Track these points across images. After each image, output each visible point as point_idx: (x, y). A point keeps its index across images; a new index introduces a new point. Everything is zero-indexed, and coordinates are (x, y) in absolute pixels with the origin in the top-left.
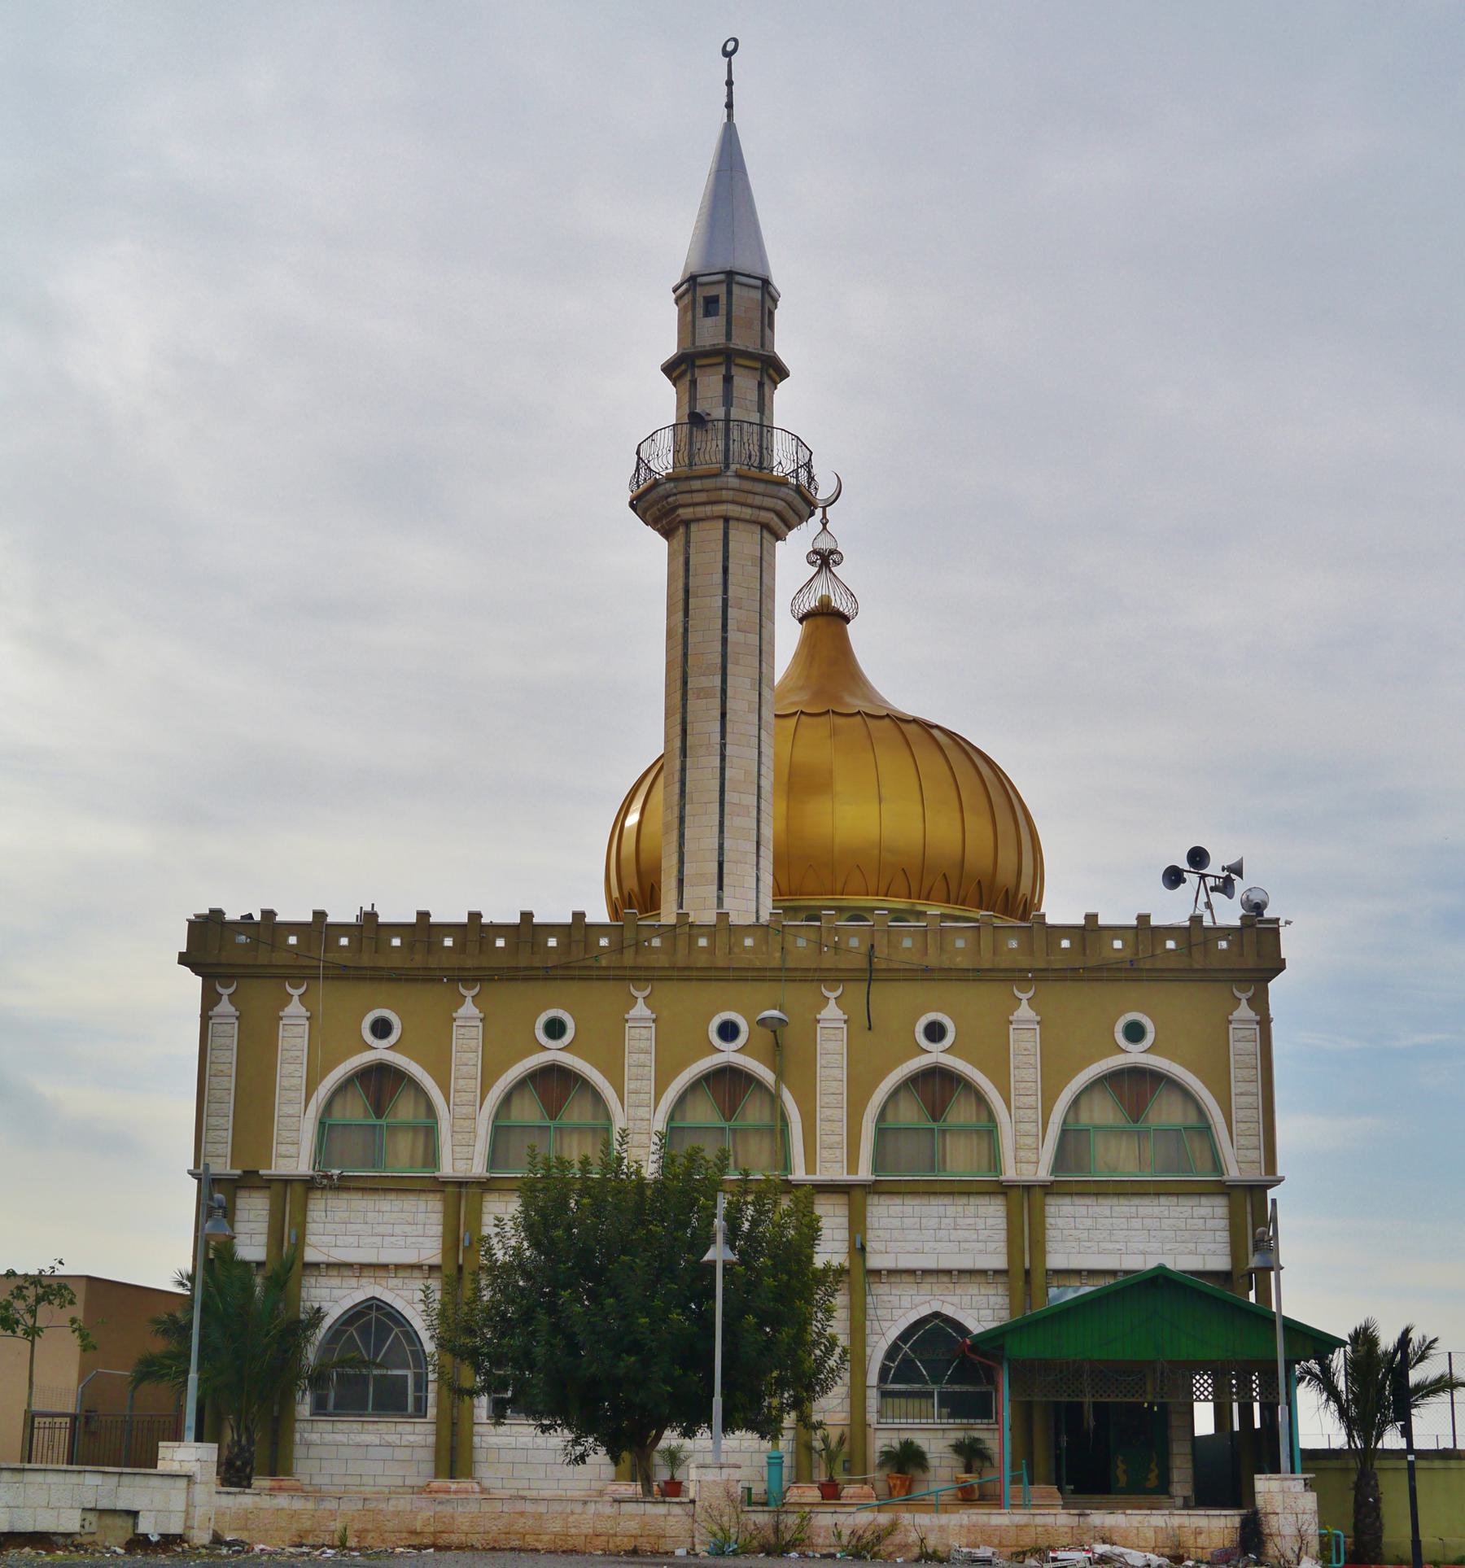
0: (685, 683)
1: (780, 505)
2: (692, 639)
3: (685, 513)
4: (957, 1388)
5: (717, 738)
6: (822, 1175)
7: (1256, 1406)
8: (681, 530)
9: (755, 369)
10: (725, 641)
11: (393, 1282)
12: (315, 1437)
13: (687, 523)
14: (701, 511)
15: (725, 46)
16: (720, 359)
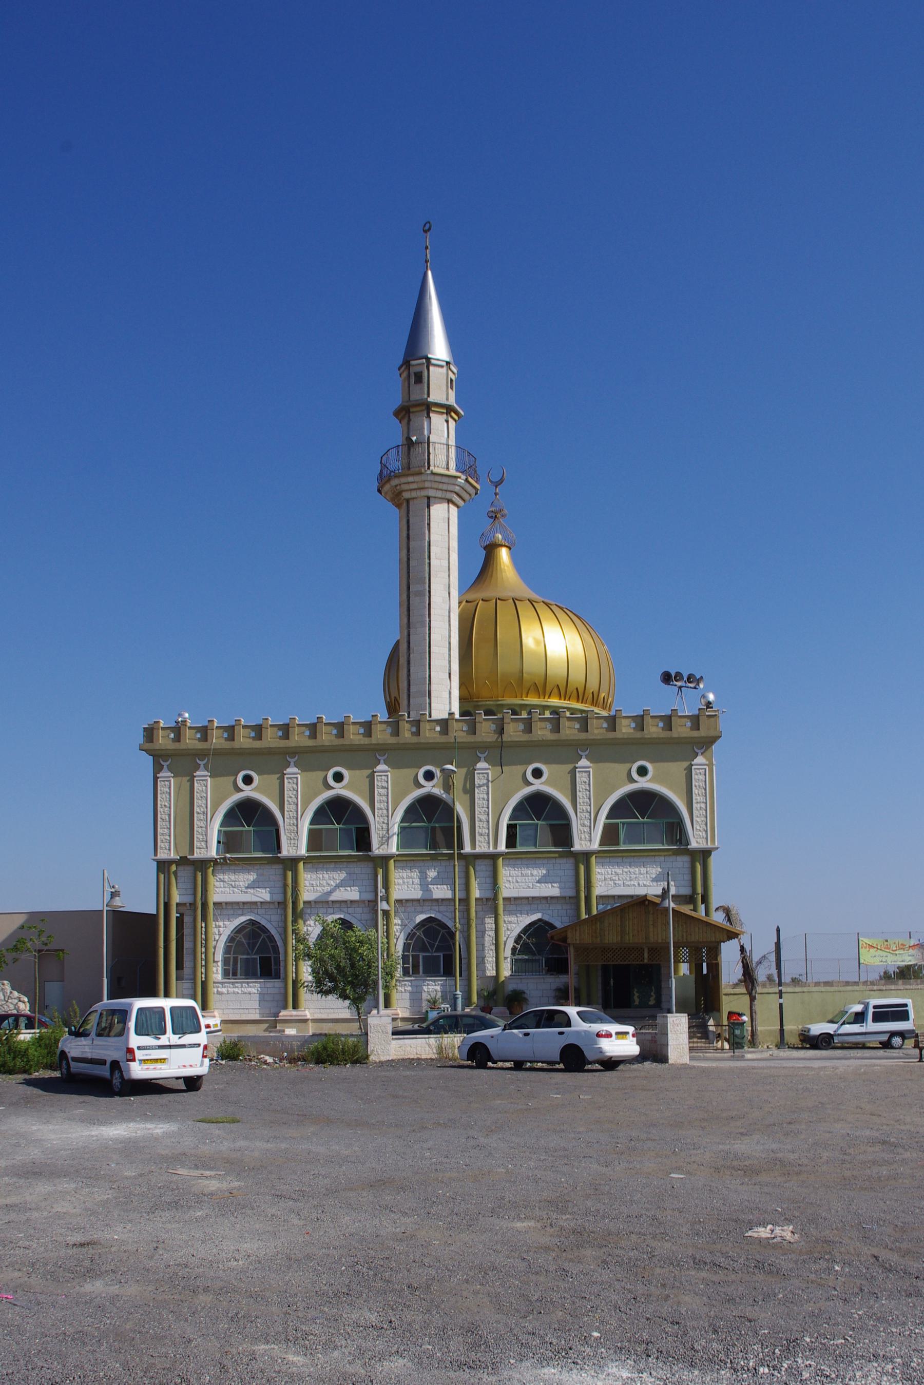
0: (409, 588)
1: (457, 489)
2: (412, 563)
3: (406, 495)
4: (520, 957)
6: (478, 850)
7: (705, 965)
8: (405, 504)
9: (443, 413)
11: (260, 911)
13: (408, 501)
14: (414, 494)
16: (424, 408)
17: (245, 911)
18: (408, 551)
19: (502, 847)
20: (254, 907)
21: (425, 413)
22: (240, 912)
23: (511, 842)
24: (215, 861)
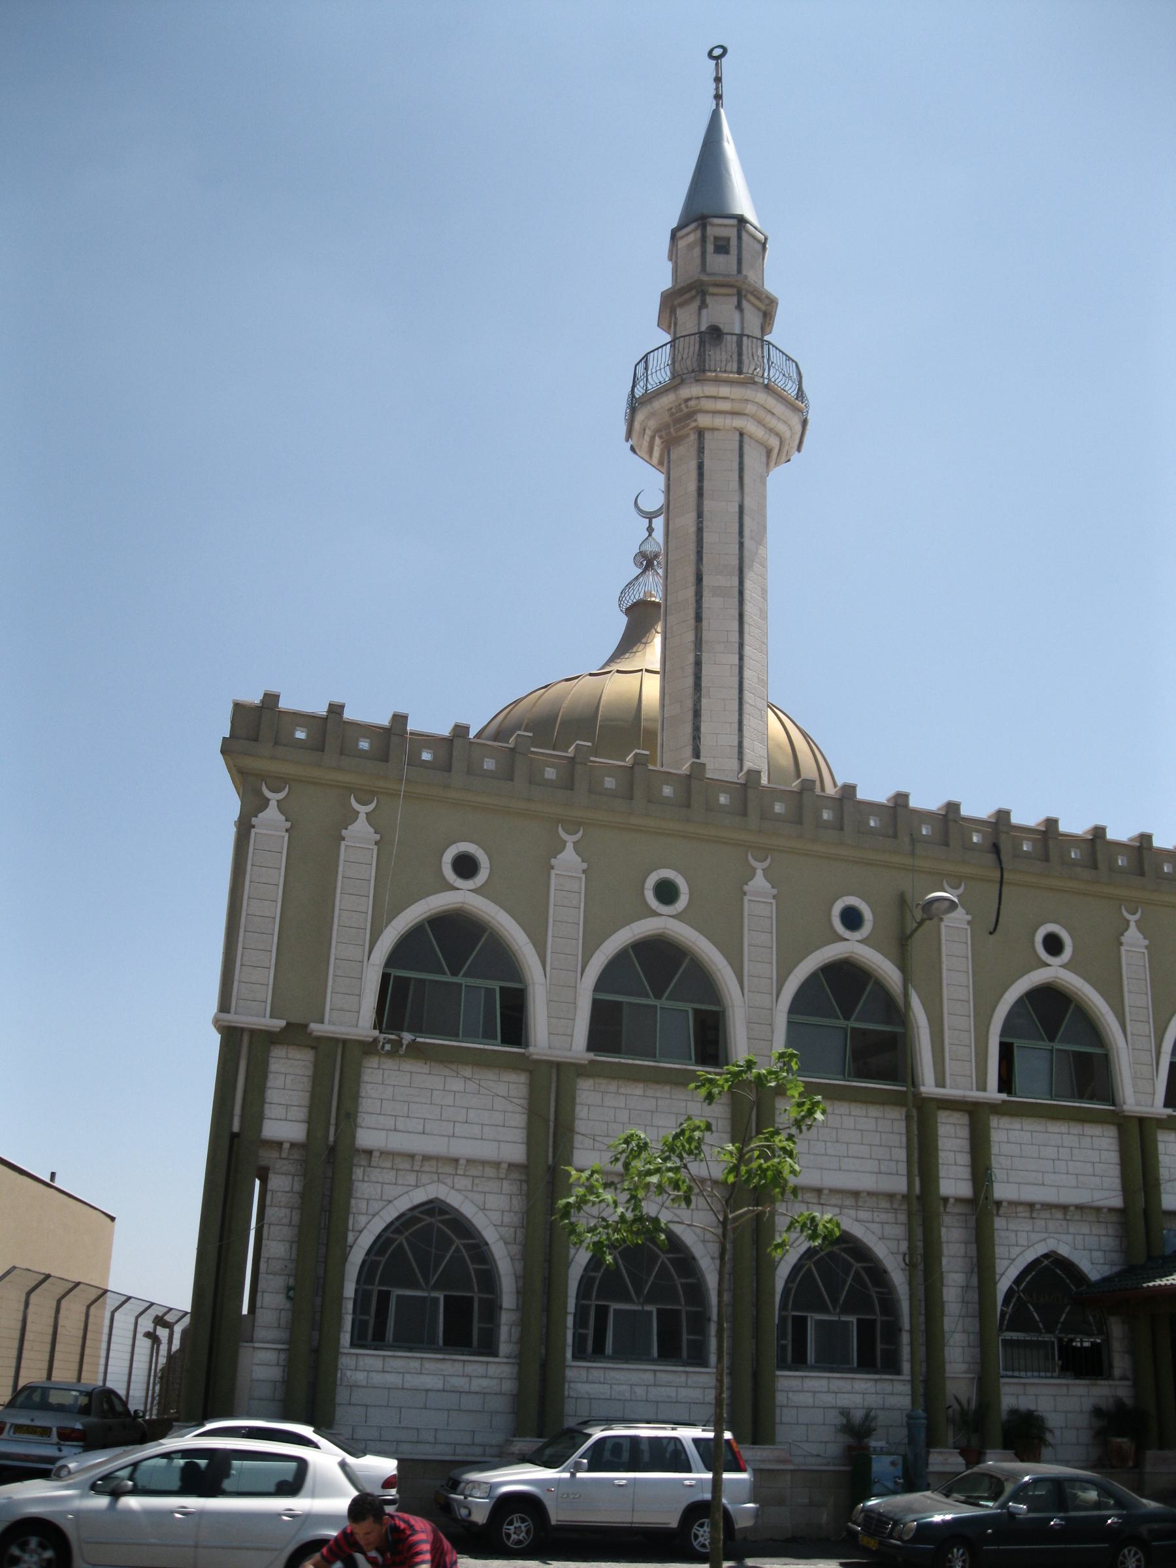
2: (707, 537)
3: (703, 421)
5: (735, 637)
6: (949, 1092)
8: (693, 437)
10: (741, 545)
11: (462, 1182)
12: (360, 1377)
13: (701, 433)
14: (719, 421)
15: (712, 50)
17: (425, 1178)
18: (700, 515)
19: (993, 1093)
20: (449, 1169)
21: (735, 300)
22: (411, 1179)
23: (1005, 1084)
24: (369, 1048)
